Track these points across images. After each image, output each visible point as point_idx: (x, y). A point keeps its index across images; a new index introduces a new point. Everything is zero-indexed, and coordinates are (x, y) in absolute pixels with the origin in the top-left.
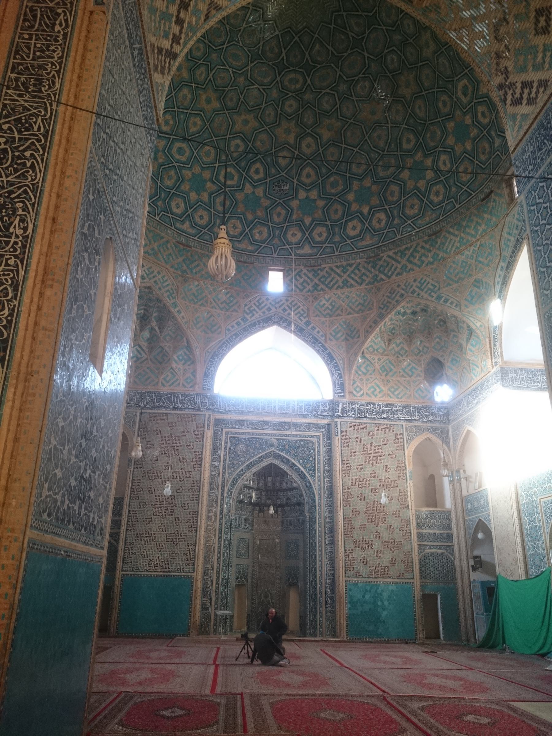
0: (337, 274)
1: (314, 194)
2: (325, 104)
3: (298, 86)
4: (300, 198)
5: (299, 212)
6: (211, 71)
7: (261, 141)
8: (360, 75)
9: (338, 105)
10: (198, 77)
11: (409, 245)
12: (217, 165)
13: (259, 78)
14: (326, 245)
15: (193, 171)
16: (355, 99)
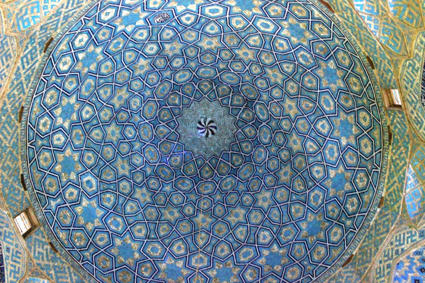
0: (71, 10)
1: (129, 29)
2: (154, 77)
3: (178, 75)
4: (141, 20)
5: (137, 13)
6: (248, 70)
7: (192, 36)
8: (142, 108)
9: (144, 82)
10: (258, 68)
11: (30, 85)
12: (228, 16)
13: (208, 70)
14: (97, 14)
15: (251, 13)
16: (136, 93)
